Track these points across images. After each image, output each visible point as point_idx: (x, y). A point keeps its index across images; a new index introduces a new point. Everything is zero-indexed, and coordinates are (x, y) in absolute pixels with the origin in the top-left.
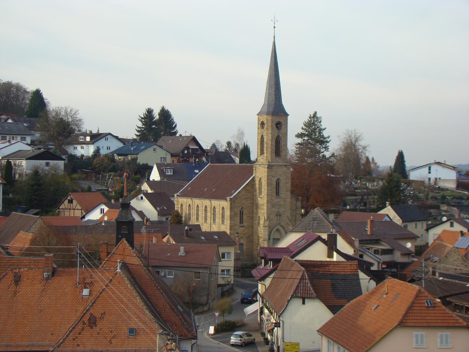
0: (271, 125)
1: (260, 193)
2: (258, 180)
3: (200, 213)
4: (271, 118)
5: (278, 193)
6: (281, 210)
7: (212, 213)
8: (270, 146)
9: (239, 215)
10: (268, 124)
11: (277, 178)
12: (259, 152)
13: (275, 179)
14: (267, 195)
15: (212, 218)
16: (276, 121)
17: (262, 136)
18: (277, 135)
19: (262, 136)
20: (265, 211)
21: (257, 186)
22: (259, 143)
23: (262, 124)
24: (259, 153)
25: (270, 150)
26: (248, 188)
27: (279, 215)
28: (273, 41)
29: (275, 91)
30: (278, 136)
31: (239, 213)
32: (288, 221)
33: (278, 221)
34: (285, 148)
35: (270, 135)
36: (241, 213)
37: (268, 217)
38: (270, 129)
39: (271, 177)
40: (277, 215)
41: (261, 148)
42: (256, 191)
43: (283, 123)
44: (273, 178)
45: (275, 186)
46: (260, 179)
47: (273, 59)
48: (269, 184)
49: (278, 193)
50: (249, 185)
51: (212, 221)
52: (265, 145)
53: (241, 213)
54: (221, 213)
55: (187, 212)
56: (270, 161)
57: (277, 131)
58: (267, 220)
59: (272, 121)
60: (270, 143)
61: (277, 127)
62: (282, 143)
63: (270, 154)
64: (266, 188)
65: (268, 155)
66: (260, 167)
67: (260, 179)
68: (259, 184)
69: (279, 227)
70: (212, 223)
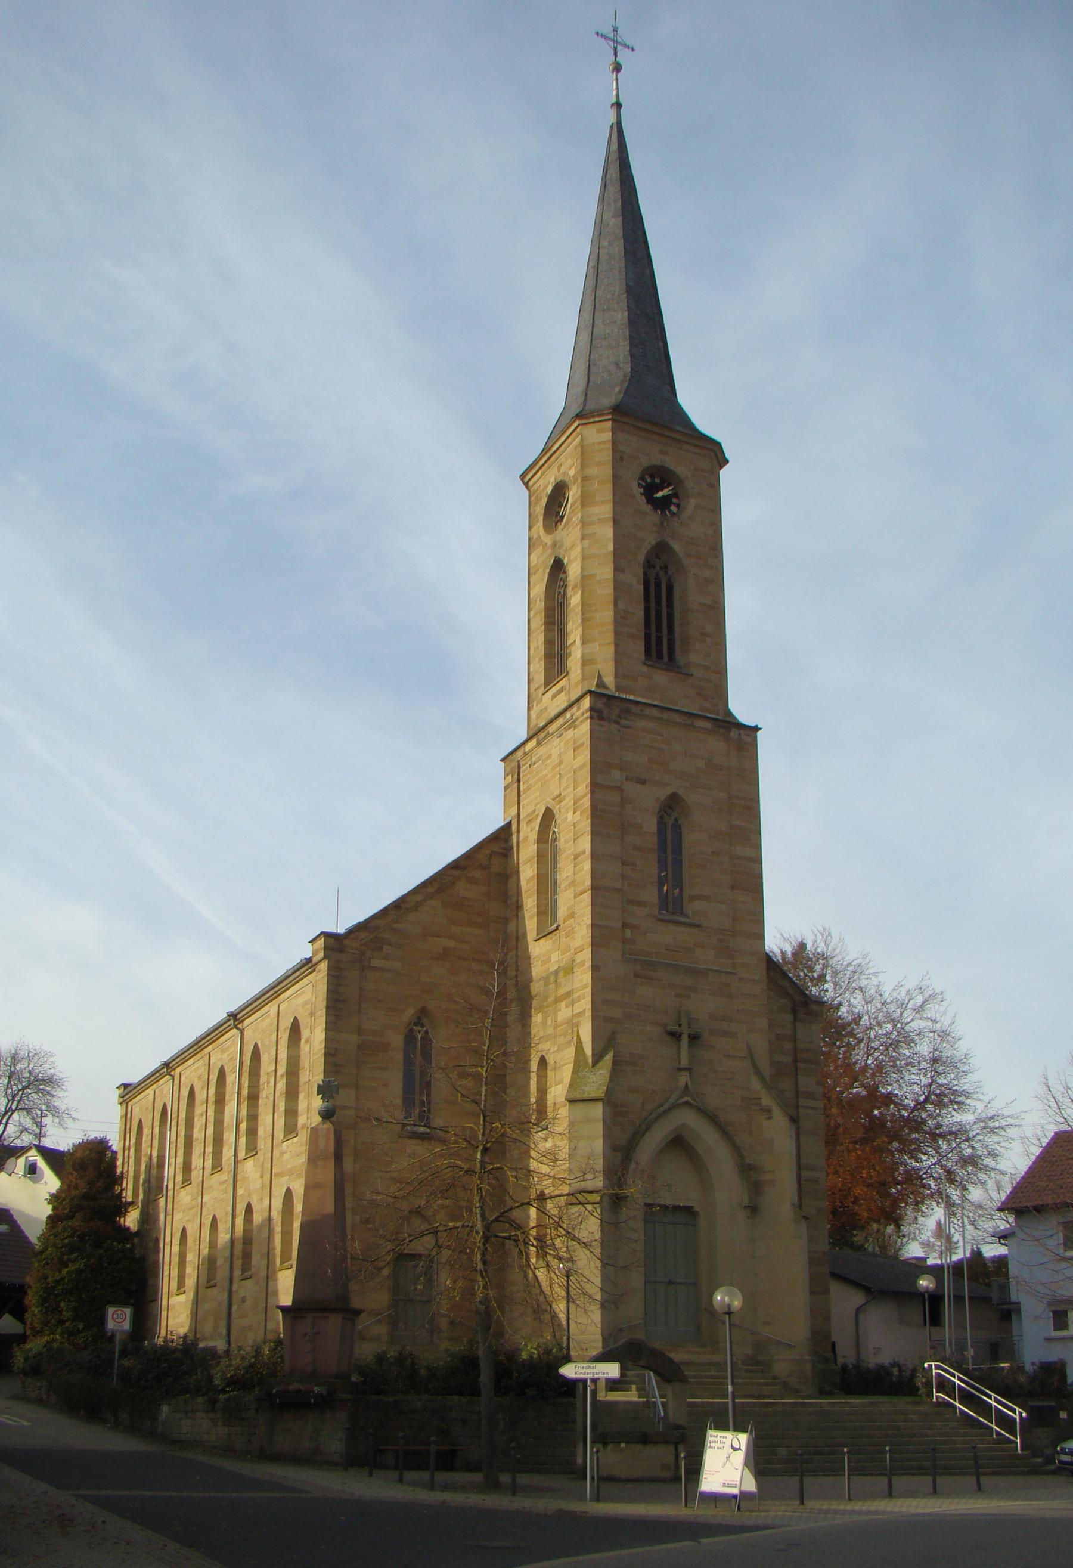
0: (607, 471)
1: (547, 910)
2: (533, 836)
3: (197, 1134)
4: (608, 436)
5: (672, 906)
6: (704, 1006)
7: (245, 1092)
8: (606, 591)
9: (399, 1057)
10: (592, 471)
11: (664, 793)
12: (539, 667)
13: (649, 798)
14: (594, 888)
15: (243, 1126)
16: (645, 462)
17: (558, 567)
18: (651, 540)
19: (558, 567)
20: (585, 1004)
21: (527, 873)
22: (539, 622)
23: (553, 508)
24: (540, 678)
25: (606, 616)
26: (463, 889)
27: (686, 1035)
28: (613, 119)
29: (631, 322)
30: (661, 549)
31: (397, 1040)
32: (756, 1084)
33: (683, 1079)
34: (709, 628)
35: (608, 532)
36: (417, 1045)
37: (607, 1038)
38: (605, 493)
39: (616, 775)
40: (675, 1036)
41: (549, 643)
42: (518, 907)
43: (689, 484)
44: (632, 788)
45: (652, 842)
46: (548, 816)
47: (614, 189)
48: (603, 819)
49: (672, 906)
50: (478, 874)
51: (243, 1141)
52: (575, 600)
53: (417, 1045)
54: (282, 1069)
55: (155, 1154)
56: (609, 680)
57: (654, 517)
58: (597, 1057)
59: (619, 458)
60: (606, 572)
61: (649, 491)
62: (689, 592)
63: (610, 638)
64: (585, 843)
65: (594, 648)
66: (542, 751)
67: (548, 816)
68: (541, 857)
69: (688, 1119)
70: (242, 1154)
